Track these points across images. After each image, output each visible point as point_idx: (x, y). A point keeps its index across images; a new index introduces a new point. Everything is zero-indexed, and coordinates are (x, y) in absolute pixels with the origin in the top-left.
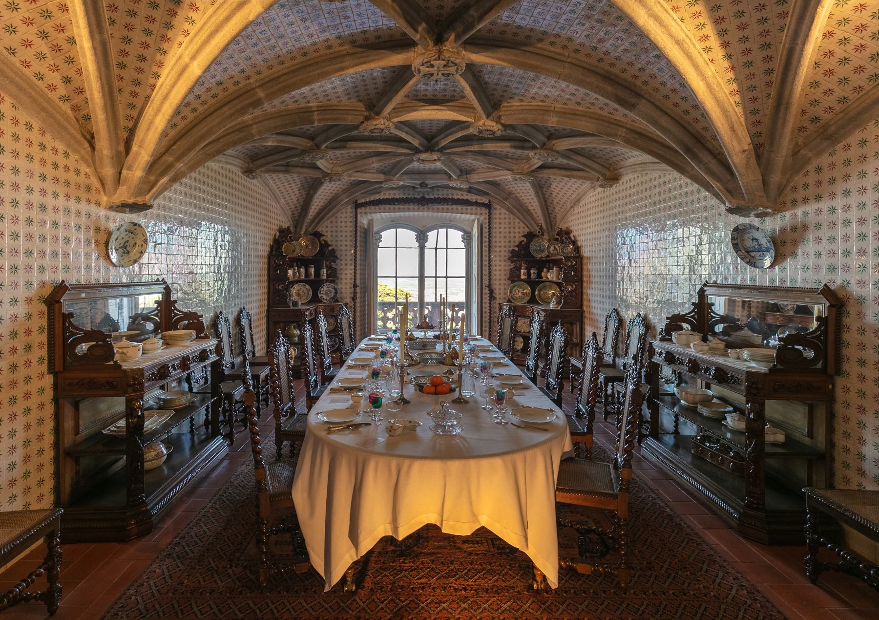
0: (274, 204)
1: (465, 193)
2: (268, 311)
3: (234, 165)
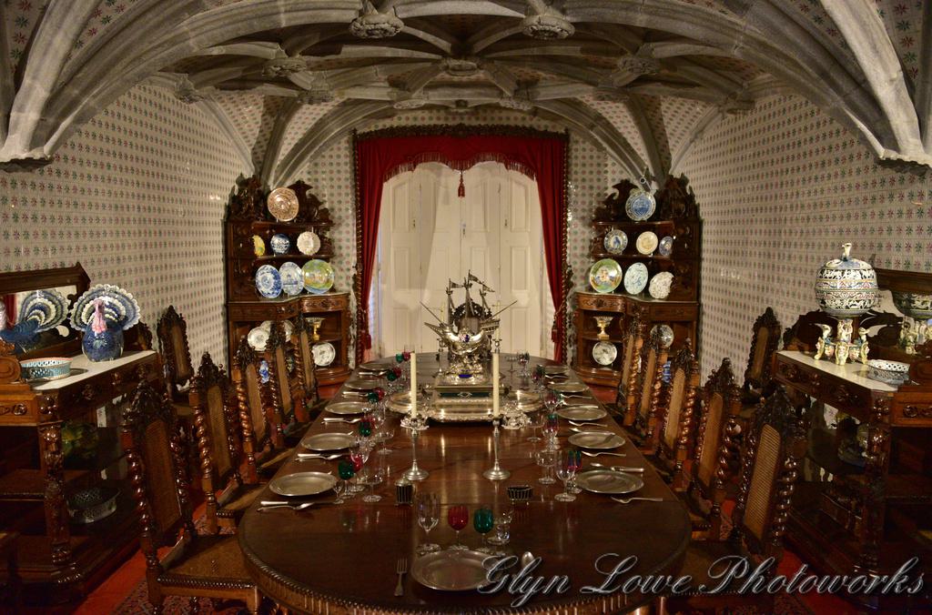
1: (528, 117)
2: (226, 306)
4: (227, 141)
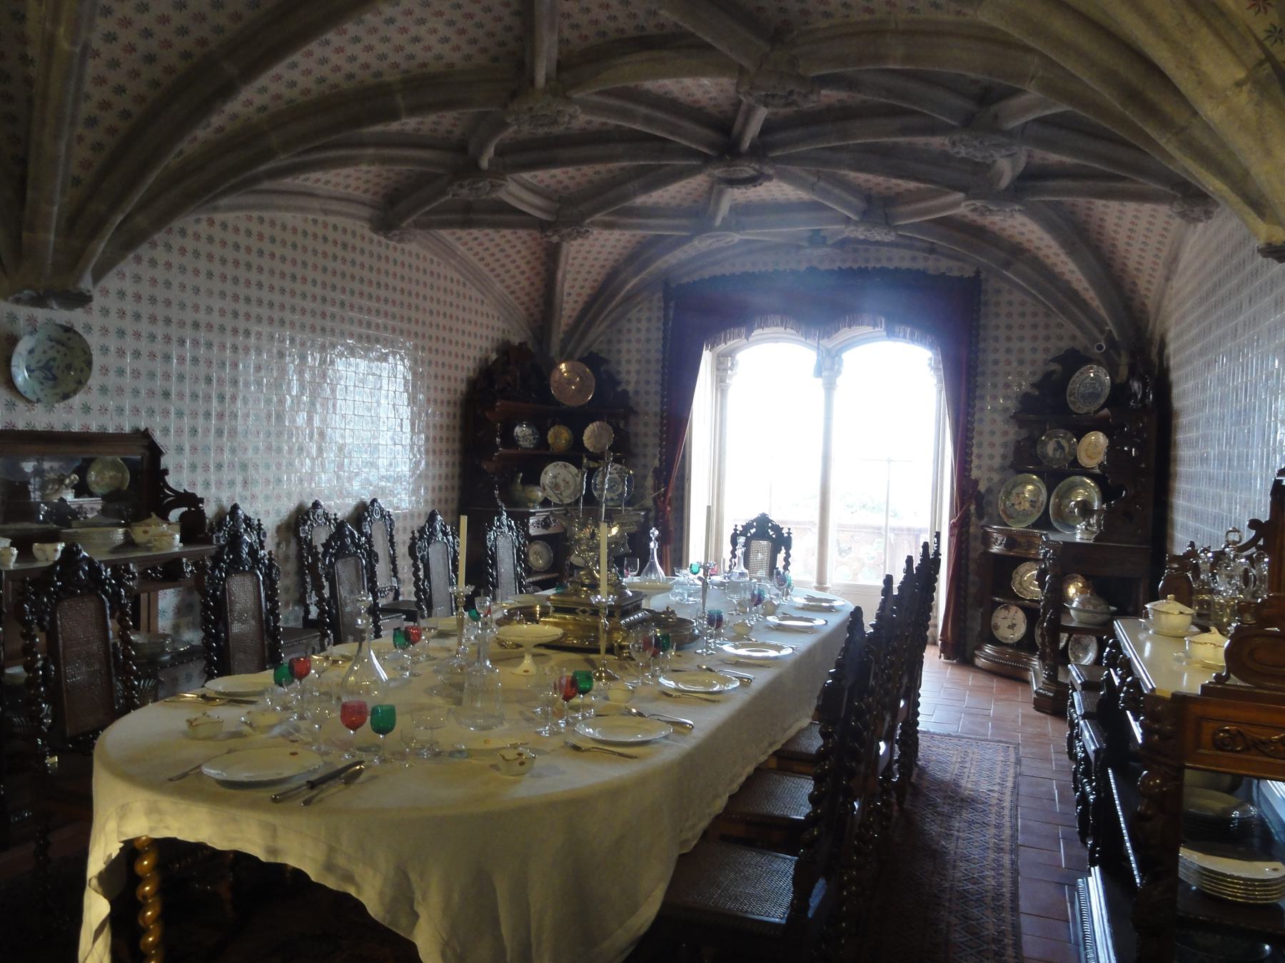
0: (474, 293)
3: (348, 215)
4: (480, 297)
